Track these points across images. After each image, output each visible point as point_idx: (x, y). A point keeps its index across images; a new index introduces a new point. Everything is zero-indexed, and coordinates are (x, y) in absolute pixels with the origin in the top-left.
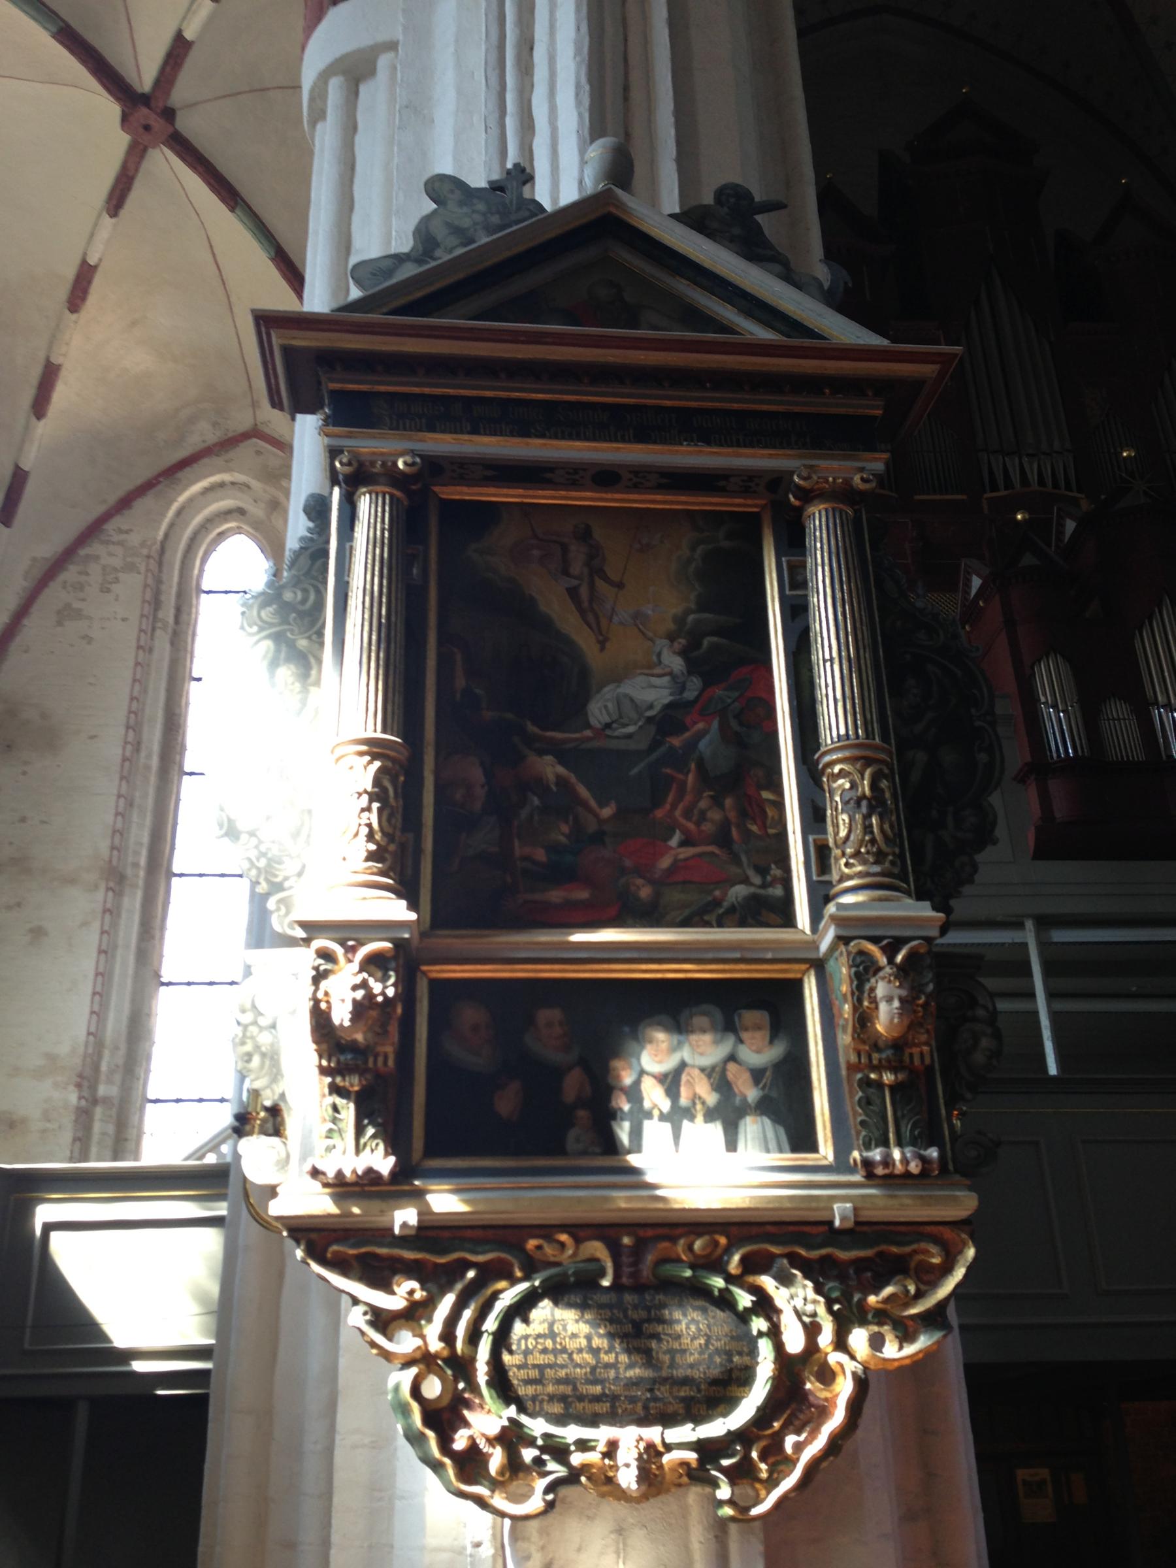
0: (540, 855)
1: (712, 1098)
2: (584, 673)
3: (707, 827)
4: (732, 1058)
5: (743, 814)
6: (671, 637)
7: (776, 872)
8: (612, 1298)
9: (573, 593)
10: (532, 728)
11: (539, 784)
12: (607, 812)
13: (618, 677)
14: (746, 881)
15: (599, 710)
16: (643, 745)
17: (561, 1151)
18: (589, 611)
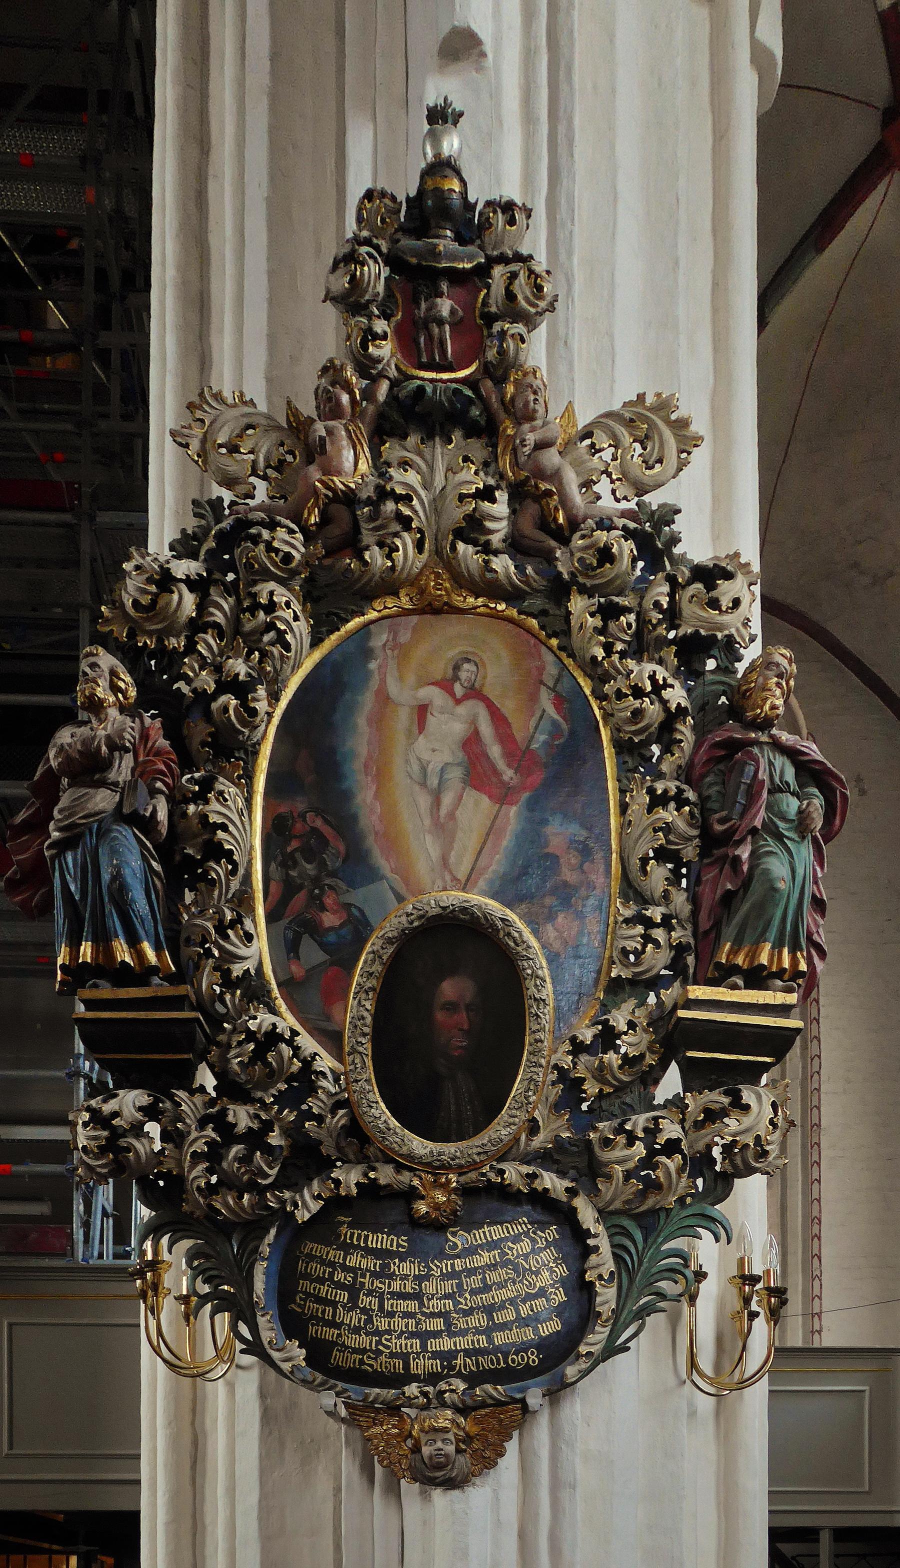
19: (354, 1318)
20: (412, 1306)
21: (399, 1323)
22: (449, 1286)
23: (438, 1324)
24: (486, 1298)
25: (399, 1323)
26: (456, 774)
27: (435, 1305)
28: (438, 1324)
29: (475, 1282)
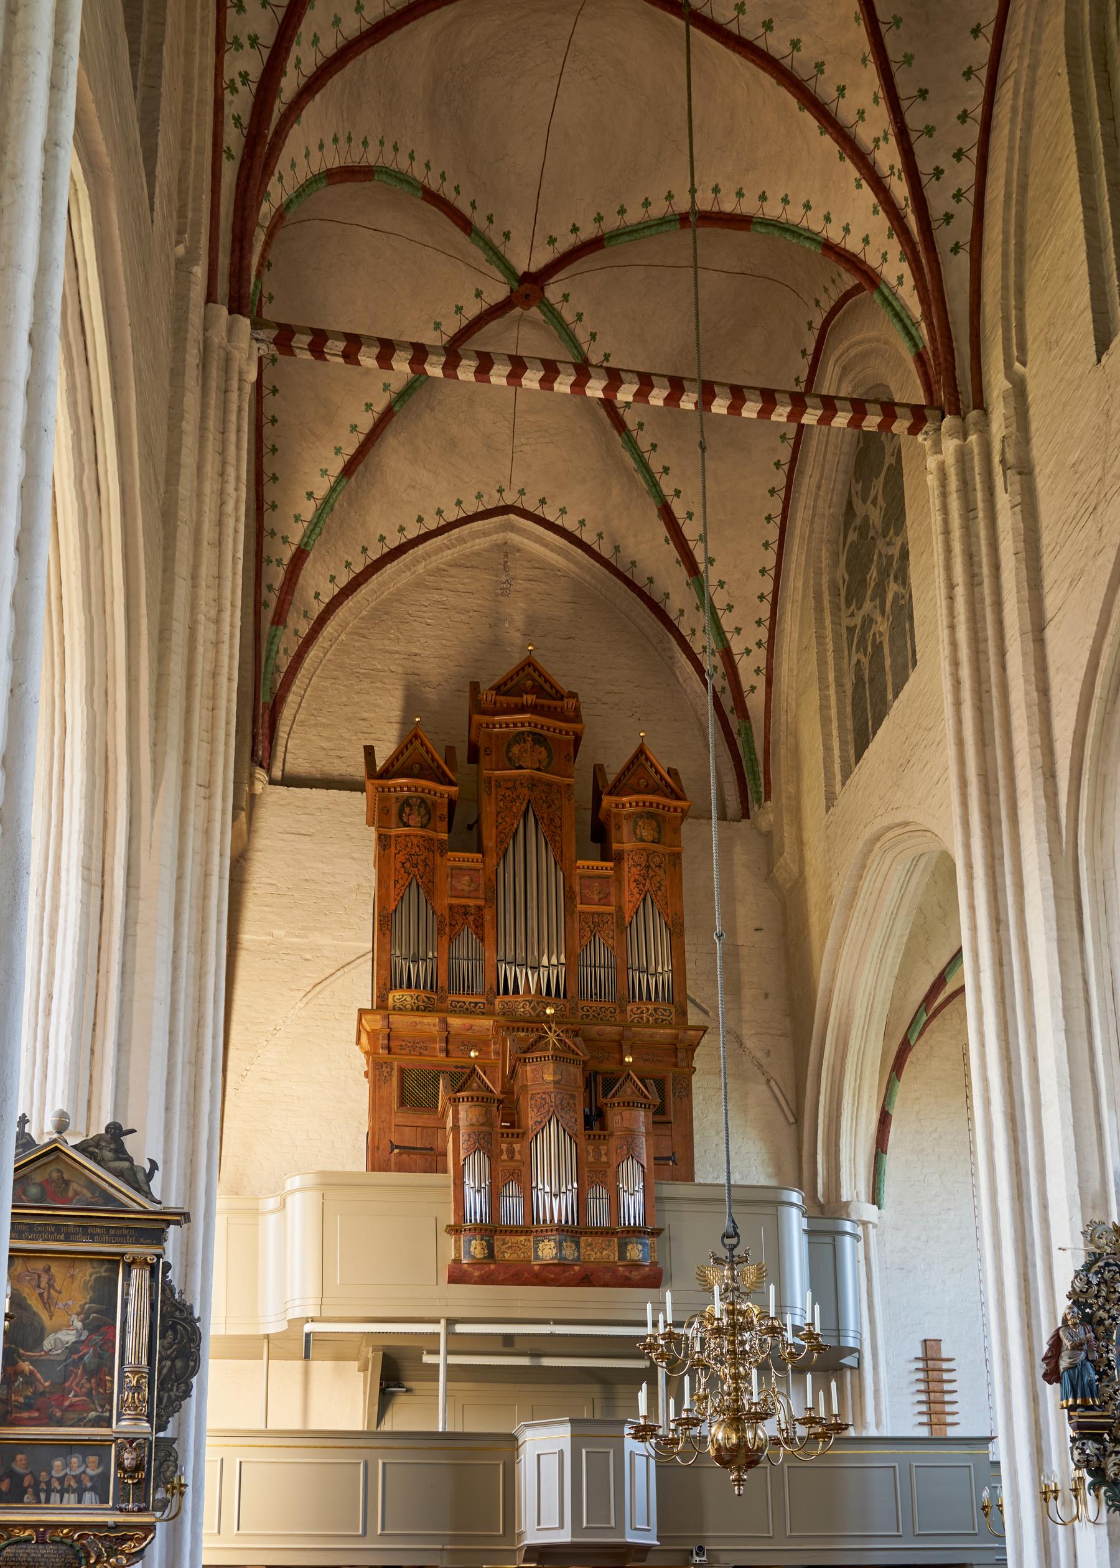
0: (22, 1400)
1: (74, 1485)
3: (84, 1390)
4: (84, 1472)
5: (98, 1385)
6: (78, 1314)
7: (107, 1407)
8: (35, 1546)
9: (41, 1295)
10: (21, 1351)
11: (22, 1373)
12: (47, 1384)
13: (56, 1331)
14: (96, 1410)
15: (47, 1344)
16: (63, 1358)
17: (22, 1502)
18: (47, 1303)
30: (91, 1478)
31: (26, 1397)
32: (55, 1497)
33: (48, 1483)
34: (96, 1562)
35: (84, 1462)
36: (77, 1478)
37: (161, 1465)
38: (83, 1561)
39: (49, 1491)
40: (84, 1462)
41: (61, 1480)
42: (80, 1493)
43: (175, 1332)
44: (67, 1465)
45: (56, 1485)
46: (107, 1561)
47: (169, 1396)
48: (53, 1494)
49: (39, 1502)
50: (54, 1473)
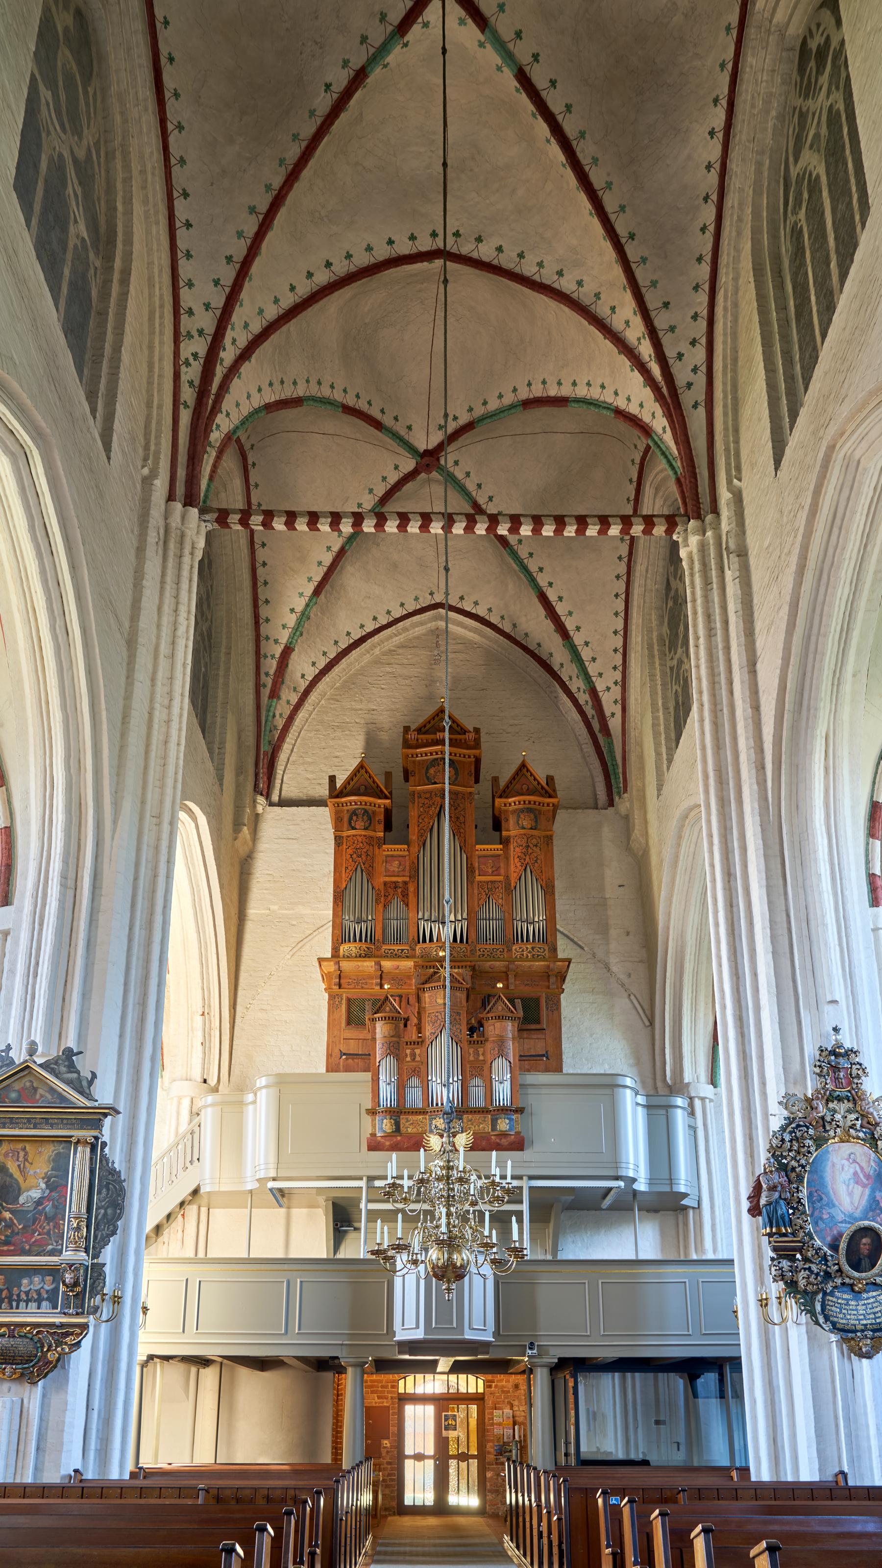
0: (3, 1238)
1: (36, 1297)
2: (19, 1189)
3: (45, 1231)
4: (42, 1288)
5: (54, 1227)
6: (43, 1178)
9: (19, 1166)
11: (5, 1220)
12: (20, 1227)
15: (22, 1200)
19: (841, 1316)
20: (855, 1312)
21: (852, 1317)
22: (864, 1307)
23: (862, 1317)
24: (873, 1310)
25: (852, 1317)
26: (852, 1181)
27: (861, 1312)
28: (862, 1317)
29: (870, 1306)
30: (47, 1292)
31: (7, 1236)
32: (22, 1304)
33: (18, 1295)
34: (48, 1350)
35: (43, 1280)
36: (38, 1292)
37: (94, 1282)
38: (39, 1350)
39: (18, 1301)
40: (43, 1280)
41: (27, 1293)
42: (39, 1301)
43: (108, 1189)
44: (31, 1283)
45: (23, 1296)
46: (55, 1350)
47: (102, 1234)
48: (21, 1303)
49: (12, 1308)
50: (23, 1289)
